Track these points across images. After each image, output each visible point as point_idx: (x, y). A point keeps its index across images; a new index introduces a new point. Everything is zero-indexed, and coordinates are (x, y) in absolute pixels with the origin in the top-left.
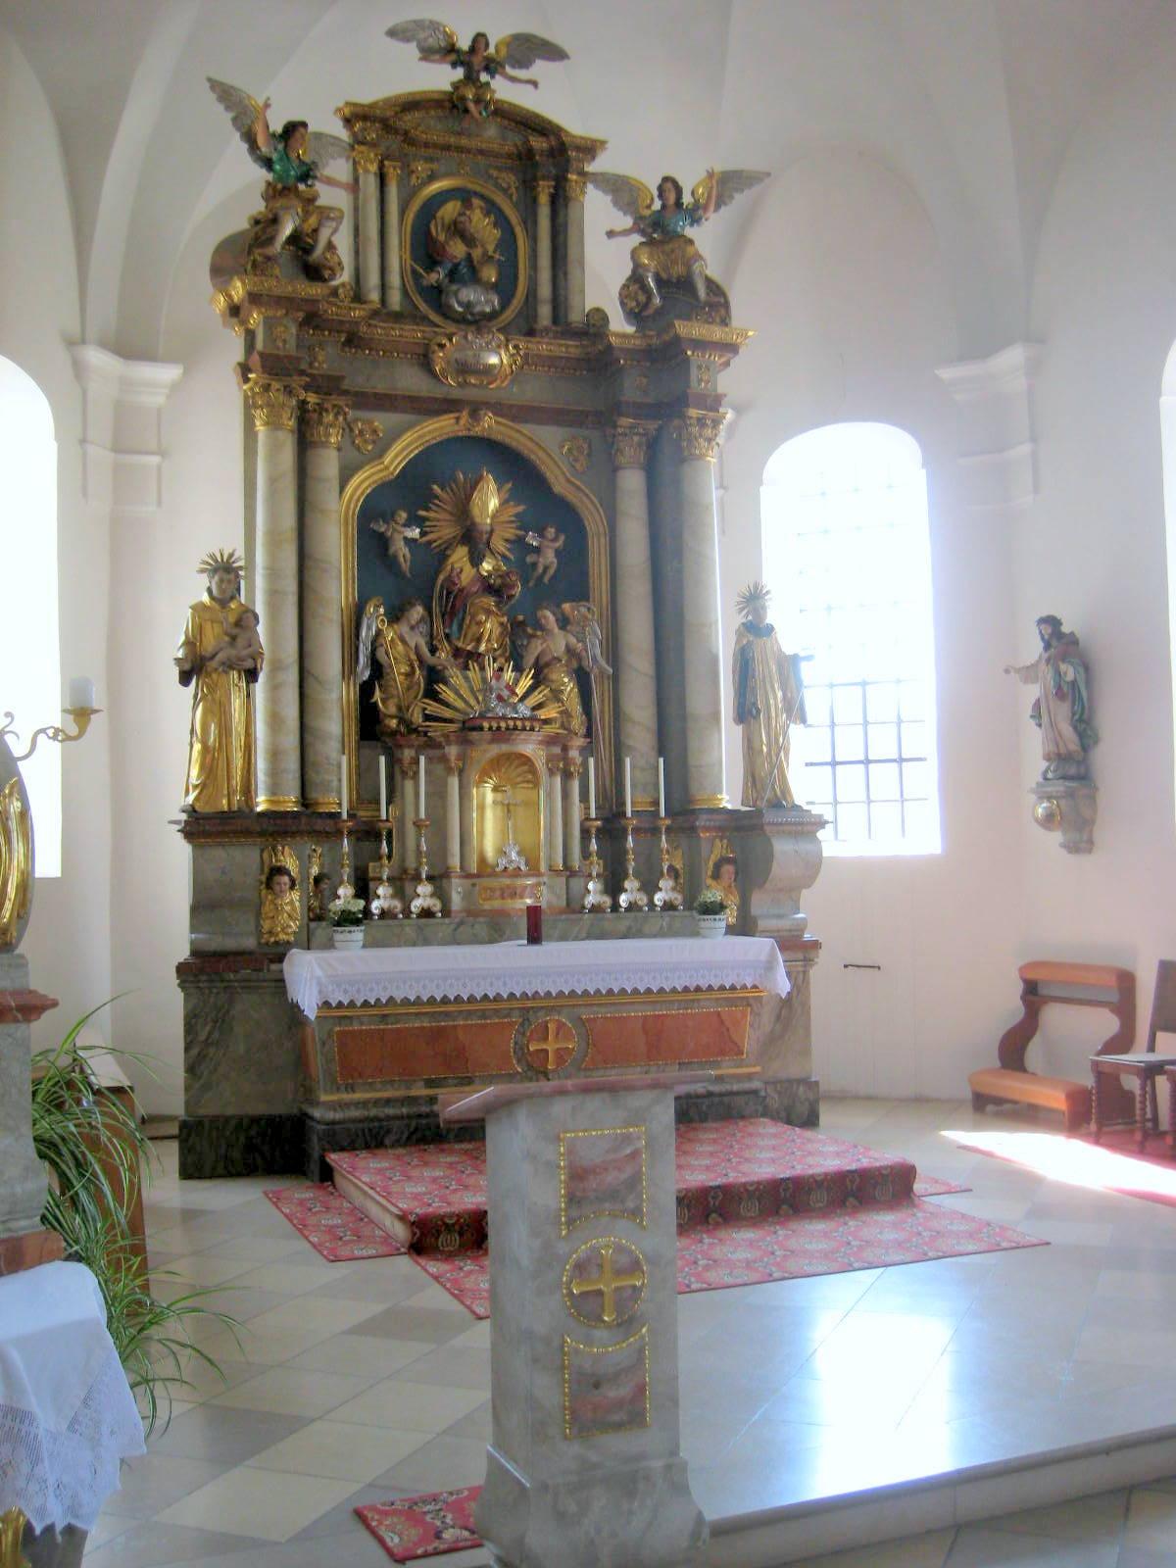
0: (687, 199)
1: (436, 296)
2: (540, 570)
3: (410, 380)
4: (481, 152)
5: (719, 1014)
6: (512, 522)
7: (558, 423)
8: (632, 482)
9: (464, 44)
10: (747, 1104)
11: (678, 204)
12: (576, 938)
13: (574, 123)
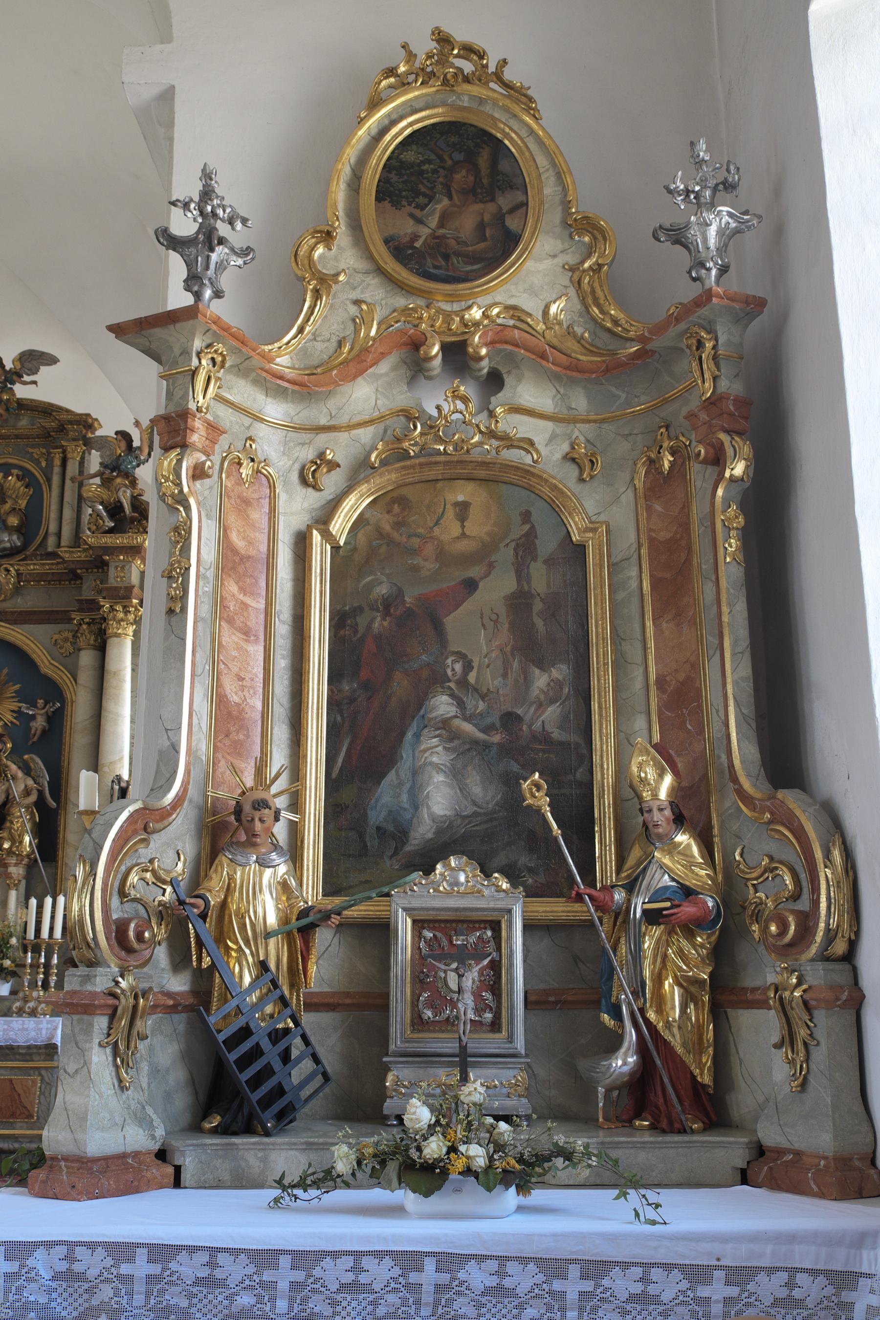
0: (136, 443)
2: (33, 732)
5: (11, 1081)
6: (13, 697)
7: (49, 622)
8: (87, 658)
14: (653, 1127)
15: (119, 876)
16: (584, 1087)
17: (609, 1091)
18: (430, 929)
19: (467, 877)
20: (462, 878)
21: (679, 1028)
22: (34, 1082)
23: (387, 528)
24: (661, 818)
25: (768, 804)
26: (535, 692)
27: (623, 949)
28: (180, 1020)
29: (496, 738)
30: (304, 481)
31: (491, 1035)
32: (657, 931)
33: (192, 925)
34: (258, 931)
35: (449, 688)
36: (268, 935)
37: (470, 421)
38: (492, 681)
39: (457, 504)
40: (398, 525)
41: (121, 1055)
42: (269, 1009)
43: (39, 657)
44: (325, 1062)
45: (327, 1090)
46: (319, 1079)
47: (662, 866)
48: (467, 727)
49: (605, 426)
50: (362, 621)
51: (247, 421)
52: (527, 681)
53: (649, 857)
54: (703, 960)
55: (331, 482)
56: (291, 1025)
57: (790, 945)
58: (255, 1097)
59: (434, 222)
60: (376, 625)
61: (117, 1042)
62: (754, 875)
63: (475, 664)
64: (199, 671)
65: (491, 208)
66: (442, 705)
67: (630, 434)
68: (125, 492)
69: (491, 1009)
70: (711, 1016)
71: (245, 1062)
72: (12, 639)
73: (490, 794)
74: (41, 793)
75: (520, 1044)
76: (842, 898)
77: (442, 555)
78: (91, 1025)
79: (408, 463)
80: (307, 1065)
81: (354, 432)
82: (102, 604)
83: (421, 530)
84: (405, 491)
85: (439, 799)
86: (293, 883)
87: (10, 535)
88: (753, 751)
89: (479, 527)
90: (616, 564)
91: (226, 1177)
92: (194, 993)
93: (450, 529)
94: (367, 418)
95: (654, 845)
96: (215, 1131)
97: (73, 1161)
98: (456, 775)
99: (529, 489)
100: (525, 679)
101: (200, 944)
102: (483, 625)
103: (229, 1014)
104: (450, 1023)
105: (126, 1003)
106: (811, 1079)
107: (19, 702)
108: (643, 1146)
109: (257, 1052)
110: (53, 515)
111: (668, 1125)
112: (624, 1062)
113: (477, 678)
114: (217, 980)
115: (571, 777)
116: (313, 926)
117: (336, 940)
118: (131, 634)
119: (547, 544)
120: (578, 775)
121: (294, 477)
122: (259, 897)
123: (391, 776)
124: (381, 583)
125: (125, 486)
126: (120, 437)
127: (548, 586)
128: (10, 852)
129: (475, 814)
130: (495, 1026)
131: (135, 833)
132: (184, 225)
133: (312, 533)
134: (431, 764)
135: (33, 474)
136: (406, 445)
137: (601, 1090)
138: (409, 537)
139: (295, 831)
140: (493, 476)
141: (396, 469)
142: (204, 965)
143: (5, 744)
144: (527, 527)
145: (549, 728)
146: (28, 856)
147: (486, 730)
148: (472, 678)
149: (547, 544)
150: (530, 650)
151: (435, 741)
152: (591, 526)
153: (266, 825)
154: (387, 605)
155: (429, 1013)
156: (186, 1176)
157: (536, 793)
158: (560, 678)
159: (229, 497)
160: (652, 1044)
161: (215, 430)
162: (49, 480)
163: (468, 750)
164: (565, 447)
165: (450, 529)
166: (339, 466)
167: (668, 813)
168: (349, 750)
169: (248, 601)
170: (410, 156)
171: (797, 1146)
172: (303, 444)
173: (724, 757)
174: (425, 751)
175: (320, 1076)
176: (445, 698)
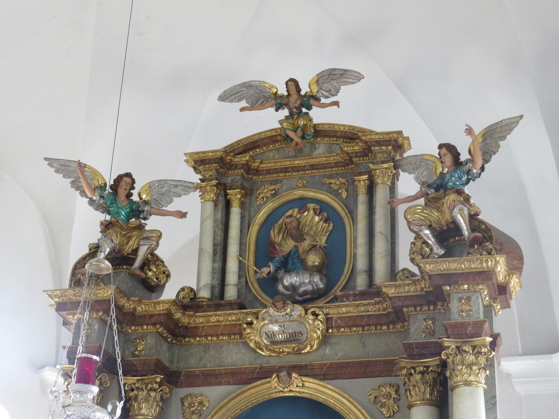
0: (464, 156)
1: (270, 284)
3: (233, 356)
4: (313, 167)
9: (283, 91)
11: (457, 163)
13: (379, 124)
68: (461, 210)
72: (321, 397)
82: (446, 344)
87: (311, 275)
110: (361, 251)
118: (483, 381)
126: (444, 150)
162: (352, 213)
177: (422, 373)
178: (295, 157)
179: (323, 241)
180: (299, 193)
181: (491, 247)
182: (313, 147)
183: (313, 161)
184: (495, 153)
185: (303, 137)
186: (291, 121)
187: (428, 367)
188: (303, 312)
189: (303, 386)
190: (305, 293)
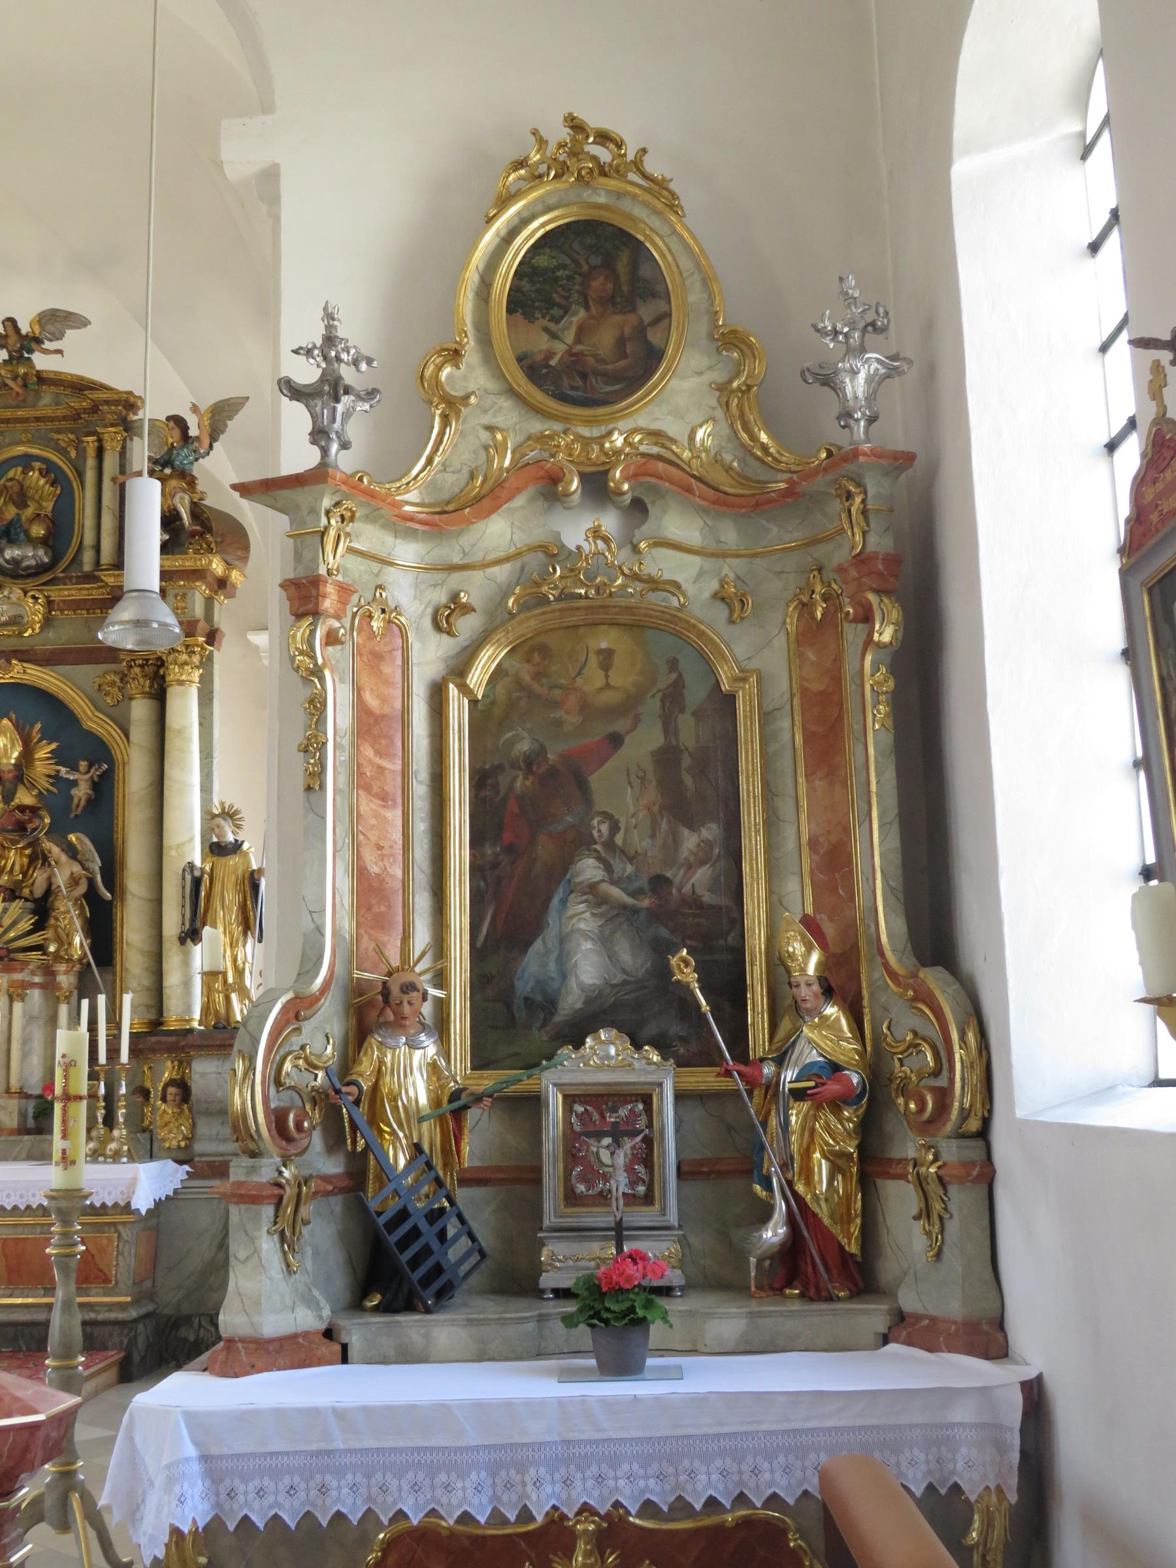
0: (193, 431)
2: (75, 801)
4: (38, 419)
6: (48, 759)
8: (140, 710)
10: (111, 1335)
11: (186, 438)
12: (15, 1159)
14: (802, 1295)
15: (275, 1066)
16: (738, 1256)
17: (760, 1261)
18: (581, 1103)
19: (617, 1050)
20: (613, 1051)
21: (826, 1200)
22: (109, 1239)
23: (527, 678)
24: (808, 993)
25: (911, 981)
26: (684, 853)
27: (773, 1122)
28: (337, 1203)
29: (645, 903)
30: (437, 627)
31: (644, 1208)
32: (805, 1106)
33: (344, 1111)
34: (411, 1113)
35: (596, 851)
36: (421, 1120)
37: (613, 563)
38: (640, 843)
39: (600, 652)
40: (538, 675)
41: (287, 1240)
42: (425, 1189)
43: (81, 707)
44: (479, 1236)
45: (483, 1266)
46: (475, 1258)
47: (810, 1041)
48: (616, 892)
49: (757, 561)
50: (503, 780)
51: (376, 567)
52: (676, 841)
53: (797, 1030)
54: (849, 1134)
55: (468, 626)
56: (446, 1204)
57: (930, 1121)
58: (416, 1276)
59: (570, 337)
60: (518, 784)
61: (283, 1230)
62: (900, 1049)
63: (622, 825)
64: (339, 846)
65: (631, 318)
66: (588, 869)
67: (782, 572)
68: (182, 498)
69: (644, 1181)
70: (859, 1188)
71: (403, 1244)
72: (44, 685)
73: (640, 961)
74: (91, 882)
75: (673, 1218)
76: (976, 1077)
77: (585, 707)
78: (259, 1214)
79: (548, 609)
80: (464, 1243)
81: (489, 570)
83: (563, 681)
84: (542, 639)
85: (589, 968)
86: (442, 1063)
87: (35, 548)
88: (901, 926)
89: (624, 677)
90: (769, 713)
91: (391, 1353)
92: (349, 1174)
93: (594, 678)
94: (502, 554)
95: (803, 1018)
96: (377, 1309)
97: (251, 1342)
98: (605, 941)
99: (677, 634)
100: (675, 840)
101: (354, 1127)
102: (630, 783)
103: (387, 1198)
104: (603, 1198)
105: (289, 1192)
106: (946, 1250)
107: (57, 764)
108: (791, 1314)
109: (415, 1233)
110: (89, 523)
111: (815, 1294)
112: (774, 1233)
113: (625, 840)
114: (372, 1163)
115: (721, 942)
116: (466, 1107)
117: (486, 1114)
118: (197, 680)
119: (695, 694)
120: (729, 939)
121: (427, 623)
122: (410, 1080)
123: (538, 945)
124: (523, 739)
125: (183, 490)
126: (171, 424)
127: (697, 741)
128: (57, 957)
129: (625, 983)
130: (648, 1199)
131: (288, 1022)
132: (307, 373)
133: (448, 688)
134: (579, 930)
135: (59, 468)
136: (545, 589)
137: (753, 1260)
138: (551, 688)
139: (442, 1007)
140: (635, 622)
141: (536, 616)
142: (359, 1149)
143: (42, 819)
144: (674, 676)
145: (699, 891)
146: (80, 960)
147: (633, 894)
148: (619, 839)
149: (695, 694)
150: (679, 809)
151: (582, 907)
152: (741, 675)
153: (414, 1007)
154: (529, 763)
155: (581, 1188)
156: (352, 1353)
157: (685, 971)
158: (710, 838)
159: (361, 655)
160: (801, 1216)
161: (345, 591)
162: (81, 475)
163: (617, 915)
164: (714, 585)
165: (594, 678)
166: (474, 610)
167: (816, 987)
168: (494, 918)
169: (384, 763)
170: (542, 261)
171: (932, 1312)
172: (435, 585)
173: (873, 927)
174: (572, 917)
175: (476, 1254)
176: (591, 861)
177: (142, 666)
178: (18, 407)
179: (49, 506)
180: (21, 449)
181: (211, 539)
182: (38, 395)
183: (38, 414)
184: (223, 432)
185: (25, 386)
186: (9, 368)
187: (147, 660)
188: (22, 595)
189: (25, 672)
190: (28, 567)
